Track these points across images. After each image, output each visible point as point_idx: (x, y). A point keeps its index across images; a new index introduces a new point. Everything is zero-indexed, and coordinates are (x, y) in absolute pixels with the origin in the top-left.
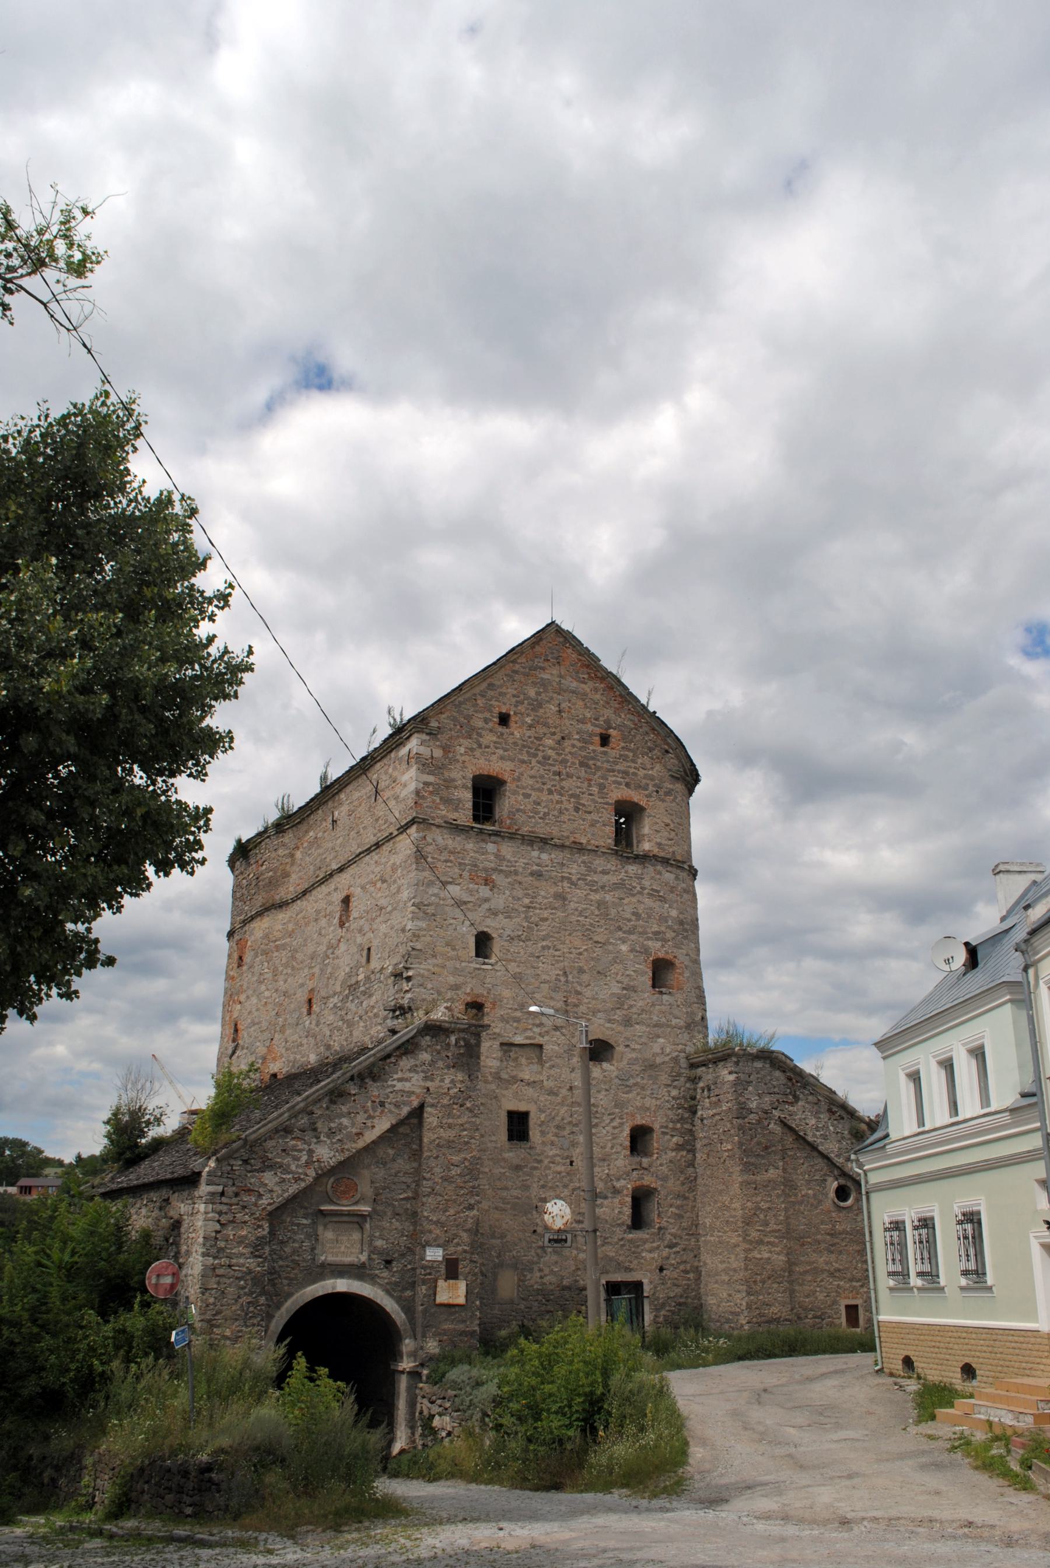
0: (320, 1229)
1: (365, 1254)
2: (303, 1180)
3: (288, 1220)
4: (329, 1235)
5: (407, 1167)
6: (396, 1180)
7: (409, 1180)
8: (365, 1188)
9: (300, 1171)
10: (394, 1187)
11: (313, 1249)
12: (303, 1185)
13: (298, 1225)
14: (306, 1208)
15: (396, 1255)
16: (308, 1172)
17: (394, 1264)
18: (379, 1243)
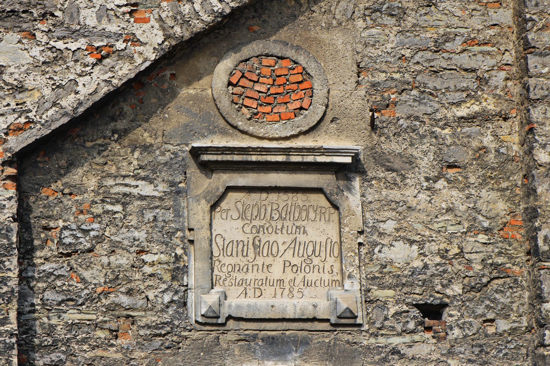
0: (198, 212)
1: (353, 286)
2: (121, 55)
3: (92, 183)
4: (229, 227)
5: (476, 22)
6: (440, 62)
7: (484, 64)
8: (337, 85)
9: (113, 28)
10: (433, 83)
11: (178, 271)
12: (125, 71)
13: (125, 200)
14: (146, 148)
15: (457, 289)
16: (138, 30)
17: (451, 315)
18: (399, 254)
